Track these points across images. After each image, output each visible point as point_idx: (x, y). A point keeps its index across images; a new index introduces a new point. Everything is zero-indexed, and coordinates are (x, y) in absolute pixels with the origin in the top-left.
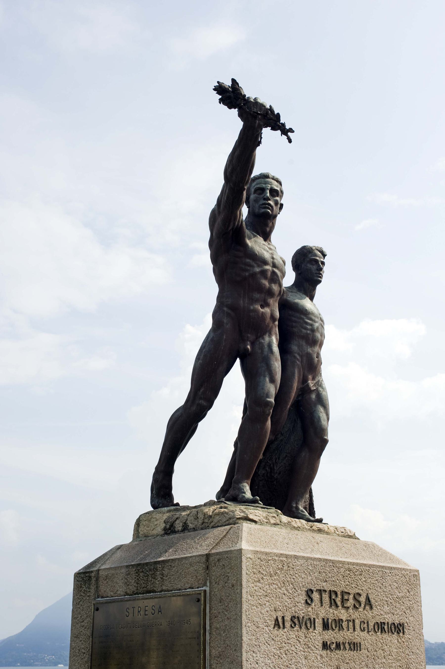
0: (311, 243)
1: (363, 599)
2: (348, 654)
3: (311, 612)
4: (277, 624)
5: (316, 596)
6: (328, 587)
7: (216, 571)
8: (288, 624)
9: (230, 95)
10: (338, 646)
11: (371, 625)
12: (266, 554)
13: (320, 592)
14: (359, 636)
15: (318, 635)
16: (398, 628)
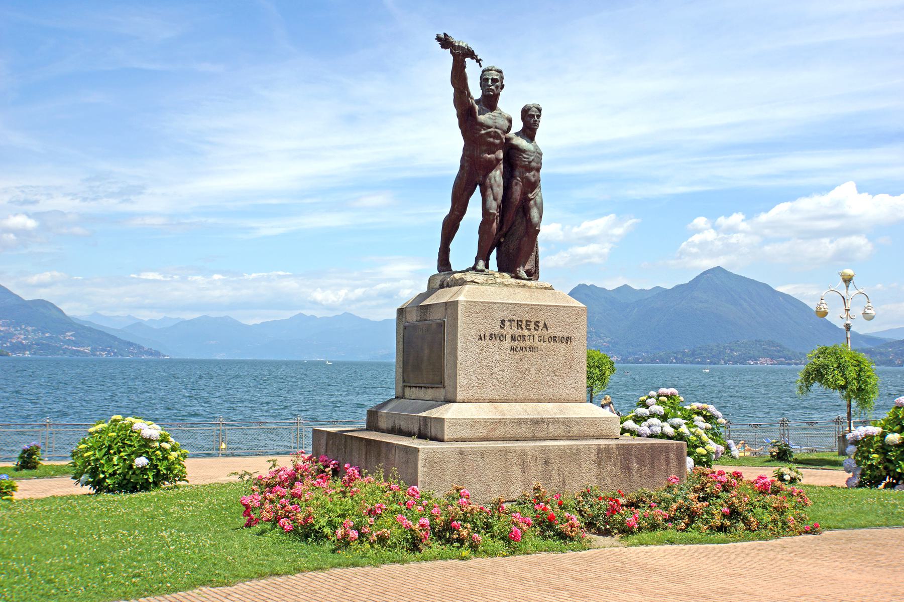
0: (530, 102)
2: (528, 354)
3: (503, 332)
4: (480, 338)
7: (449, 311)
8: (488, 338)
10: (521, 349)
11: (546, 338)
13: (510, 321)
15: (508, 343)
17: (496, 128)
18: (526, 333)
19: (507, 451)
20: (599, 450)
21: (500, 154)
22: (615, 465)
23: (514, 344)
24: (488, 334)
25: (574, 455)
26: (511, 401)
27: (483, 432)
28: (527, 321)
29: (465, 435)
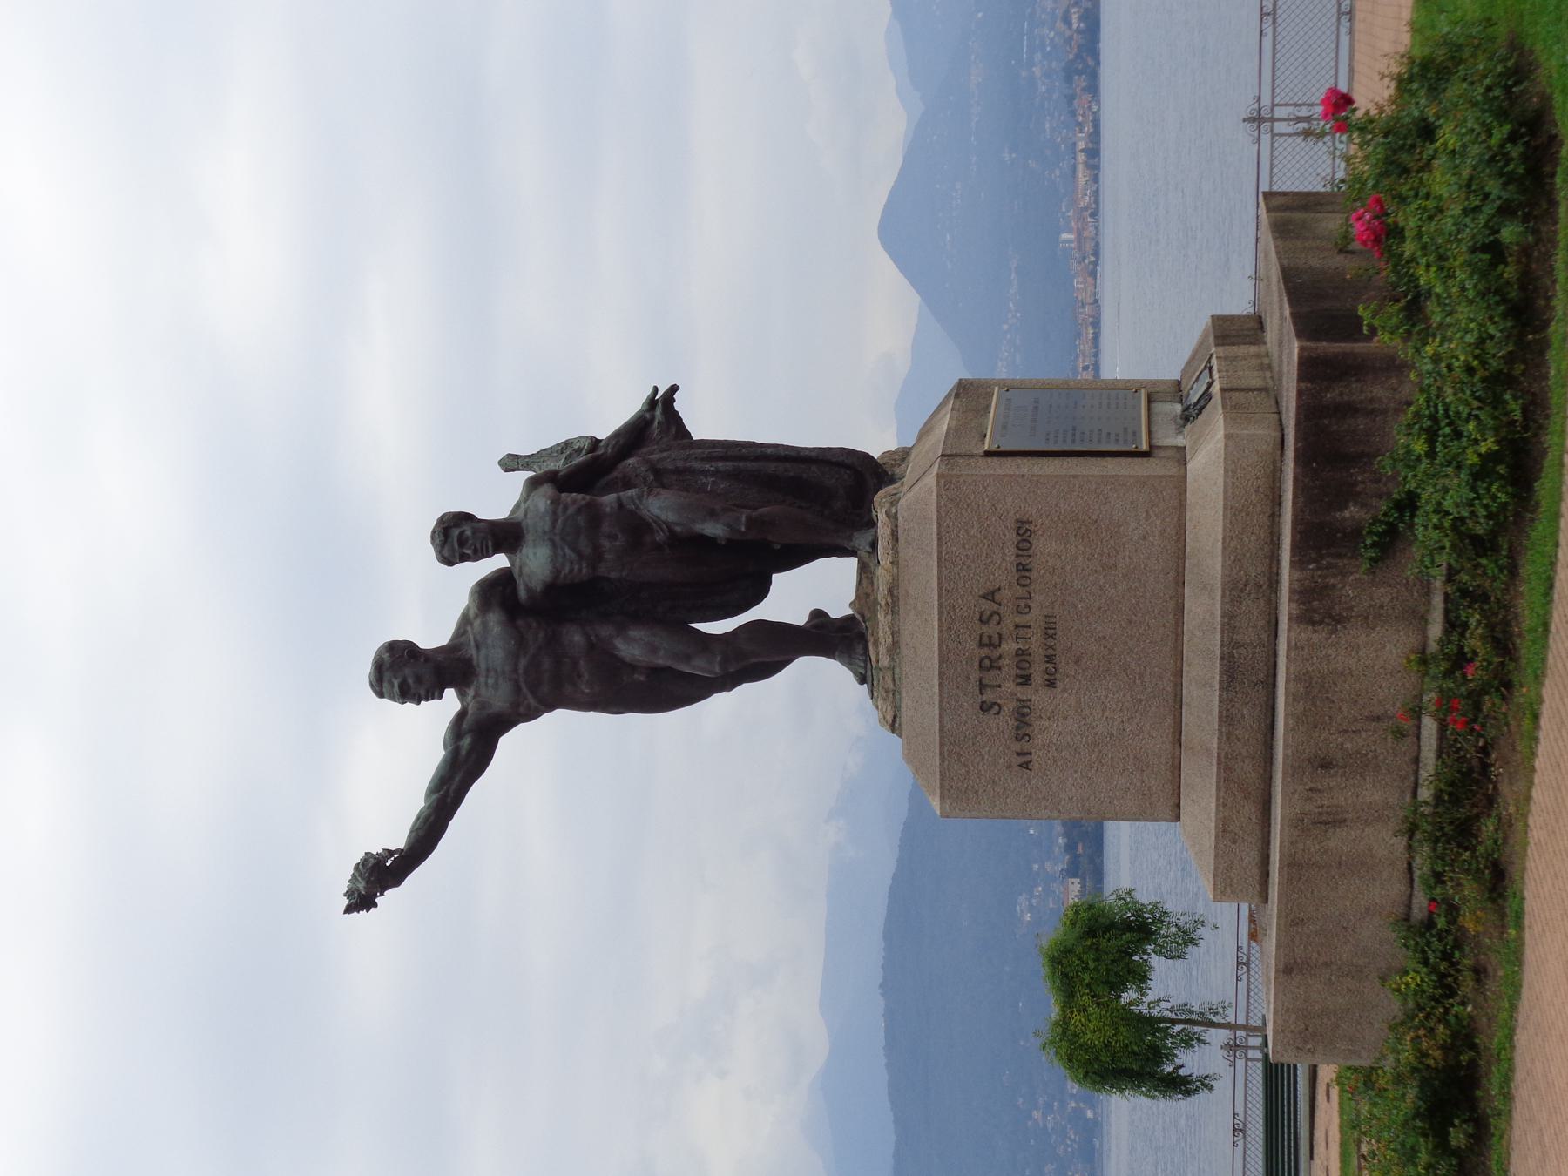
1: (988, 606)
3: (1009, 707)
4: (1026, 766)
5: (988, 696)
6: (975, 676)
9: (361, 901)
12: (942, 779)
13: (982, 687)
14: (1035, 616)
15: (1039, 697)
16: (1024, 533)
17: (515, 670)
18: (1009, 647)
19: (1292, 864)
20: (1305, 618)
21: (575, 638)
22: (1343, 574)
23: (1038, 678)
24: (1017, 746)
25: (1312, 689)
26: (1178, 686)
27: (1249, 811)
28: (981, 645)
29: (1251, 856)
